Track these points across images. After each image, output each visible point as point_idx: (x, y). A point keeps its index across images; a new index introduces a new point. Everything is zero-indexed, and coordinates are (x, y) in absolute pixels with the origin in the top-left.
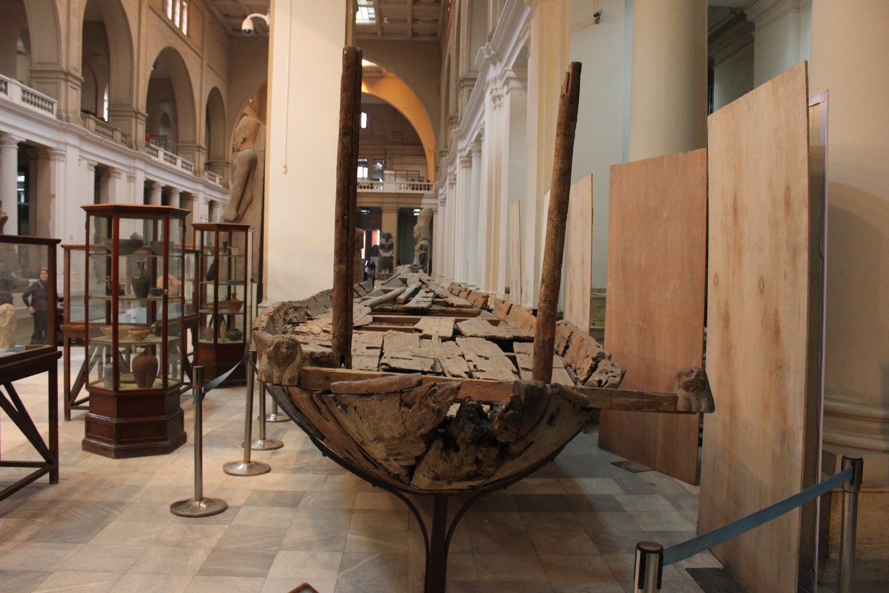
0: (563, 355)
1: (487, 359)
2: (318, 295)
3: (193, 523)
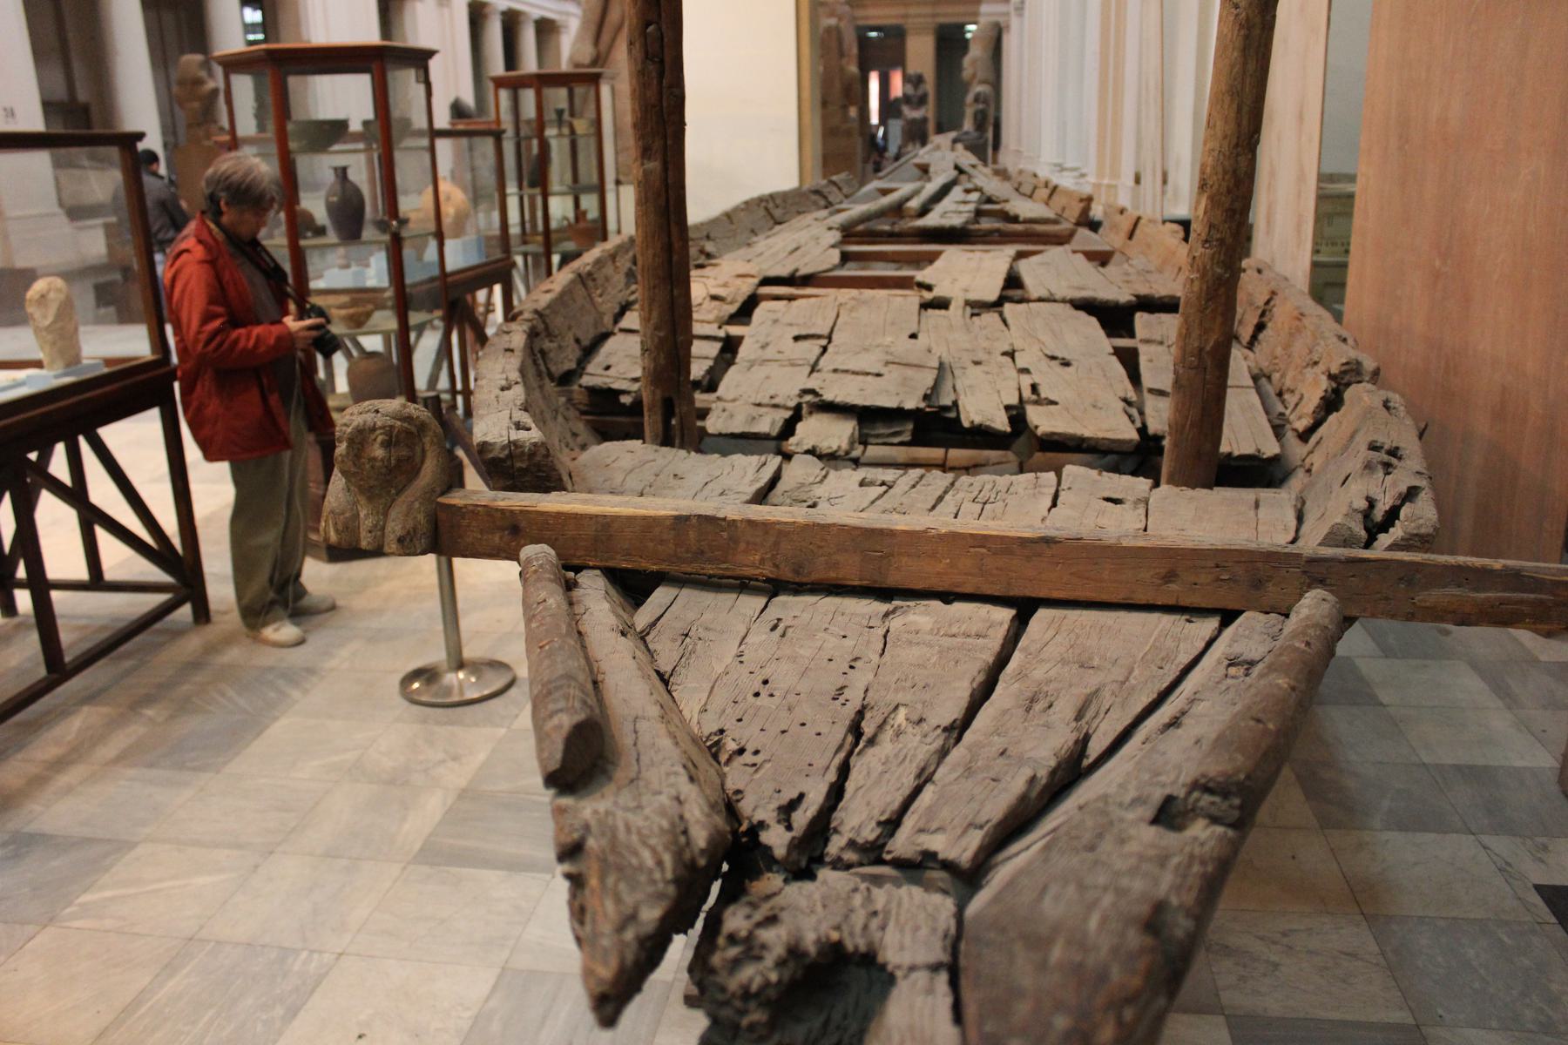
0: (1250, 346)
1: (1066, 364)
2: (736, 209)
3: (438, 723)
